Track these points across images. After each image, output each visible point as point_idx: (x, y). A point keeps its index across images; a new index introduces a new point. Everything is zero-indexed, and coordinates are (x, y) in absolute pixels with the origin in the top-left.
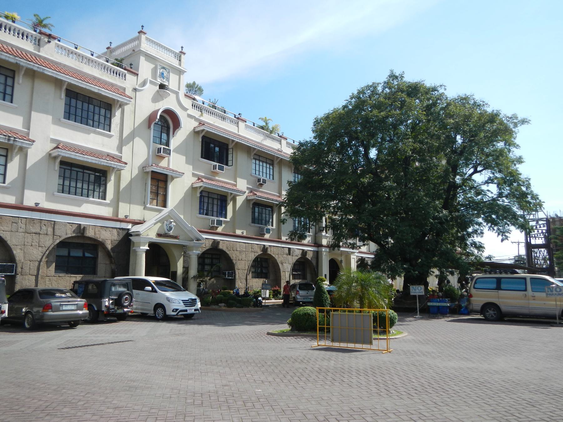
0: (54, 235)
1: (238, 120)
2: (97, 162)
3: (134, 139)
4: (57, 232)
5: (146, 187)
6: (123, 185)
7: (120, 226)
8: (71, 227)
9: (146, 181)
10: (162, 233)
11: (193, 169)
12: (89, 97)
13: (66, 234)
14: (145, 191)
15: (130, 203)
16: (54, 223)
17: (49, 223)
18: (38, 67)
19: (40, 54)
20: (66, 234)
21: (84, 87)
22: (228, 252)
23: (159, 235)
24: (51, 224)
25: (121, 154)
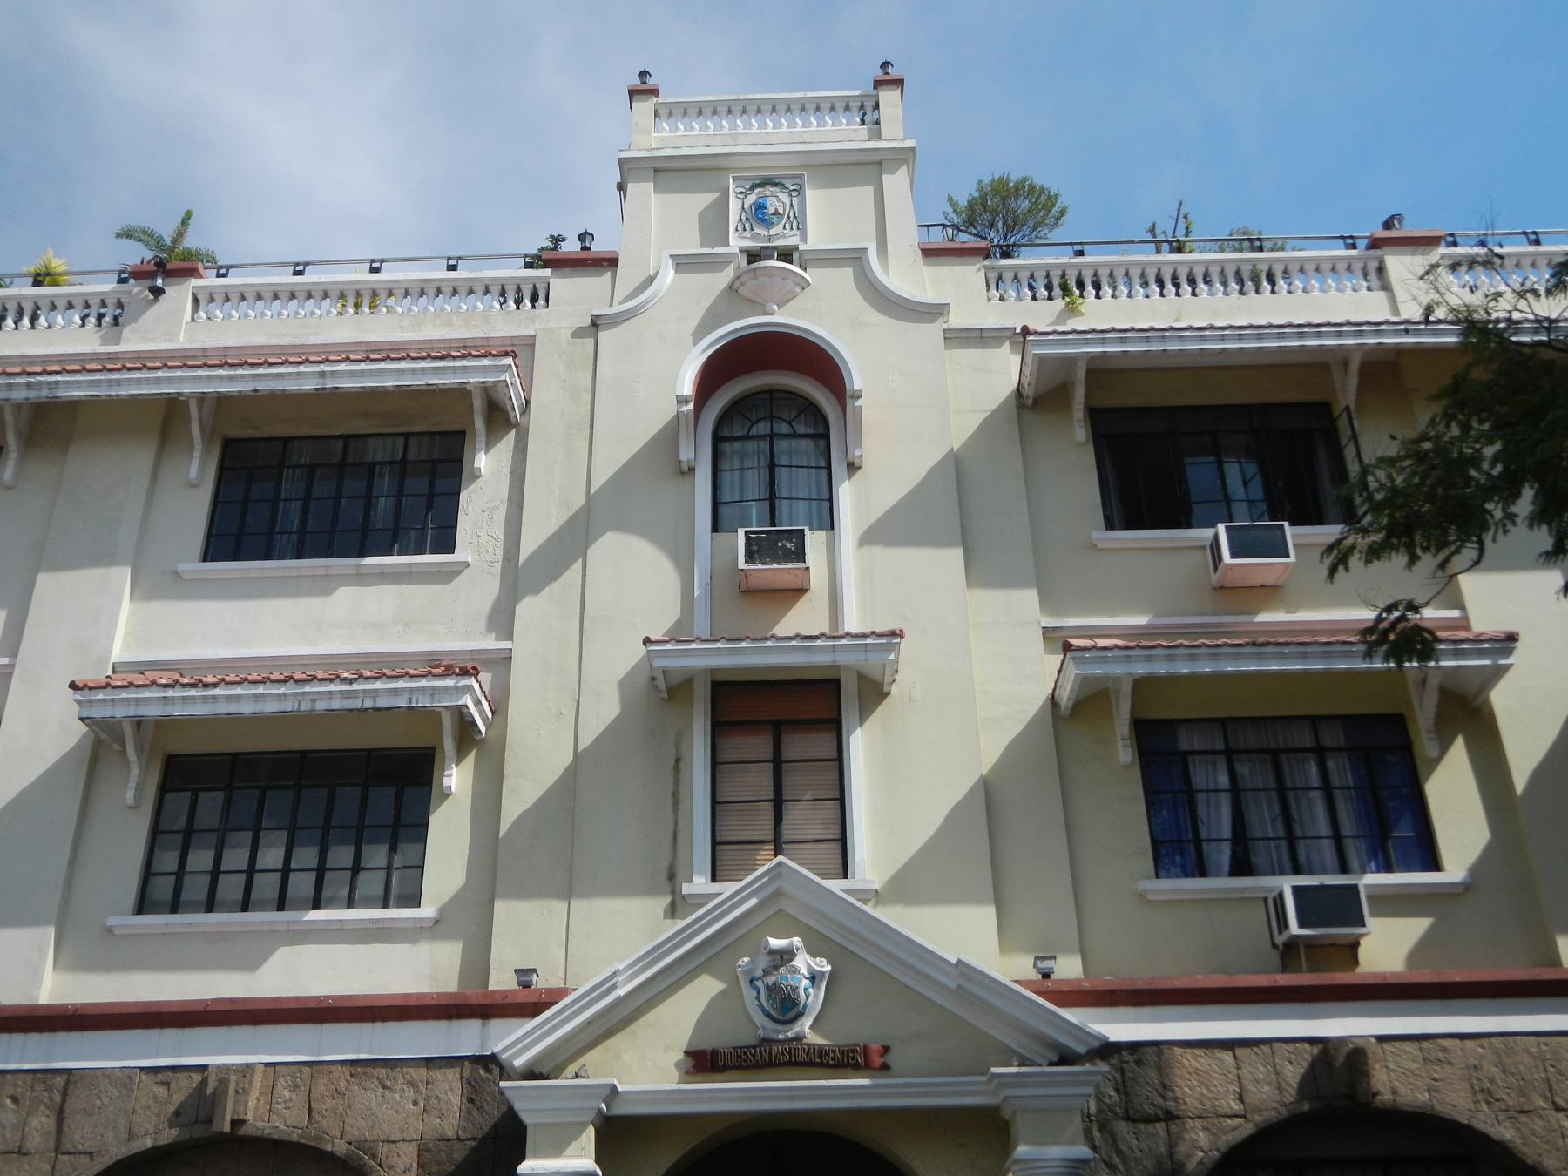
0: (58, 1149)
1: (1378, 252)
2: (288, 706)
3: (587, 548)
4: (80, 1134)
5: (677, 782)
6: (515, 804)
7: (483, 1044)
8: (161, 1091)
9: (678, 746)
10: (727, 1037)
11: (1048, 602)
12: (346, 438)
13: (131, 1135)
14: (676, 804)
15: (568, 892)
16: (68, 1081)
17: (40, 1087)
18: (29, 386)
19: (122, 347)
20: (131, 1135)
21: (247, 388)
22: (1505, 1132)
23: (703, 1062)
24: (50, 1090)
25: (509, 636)
